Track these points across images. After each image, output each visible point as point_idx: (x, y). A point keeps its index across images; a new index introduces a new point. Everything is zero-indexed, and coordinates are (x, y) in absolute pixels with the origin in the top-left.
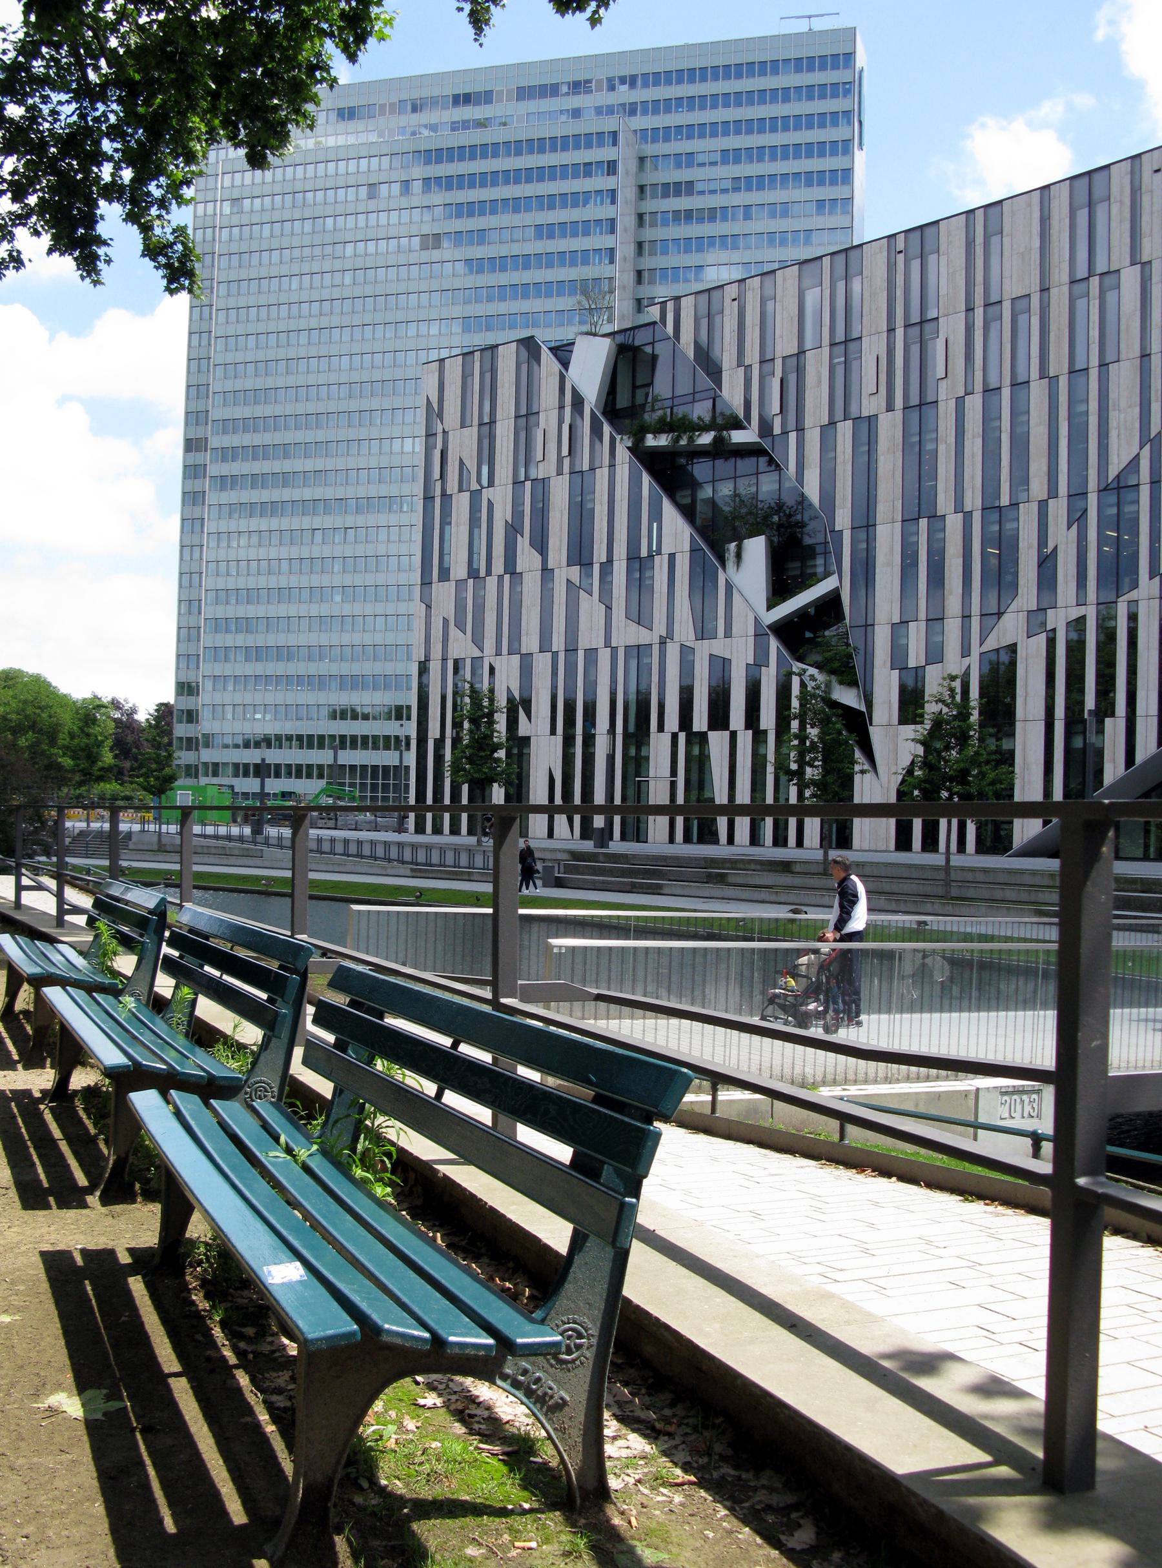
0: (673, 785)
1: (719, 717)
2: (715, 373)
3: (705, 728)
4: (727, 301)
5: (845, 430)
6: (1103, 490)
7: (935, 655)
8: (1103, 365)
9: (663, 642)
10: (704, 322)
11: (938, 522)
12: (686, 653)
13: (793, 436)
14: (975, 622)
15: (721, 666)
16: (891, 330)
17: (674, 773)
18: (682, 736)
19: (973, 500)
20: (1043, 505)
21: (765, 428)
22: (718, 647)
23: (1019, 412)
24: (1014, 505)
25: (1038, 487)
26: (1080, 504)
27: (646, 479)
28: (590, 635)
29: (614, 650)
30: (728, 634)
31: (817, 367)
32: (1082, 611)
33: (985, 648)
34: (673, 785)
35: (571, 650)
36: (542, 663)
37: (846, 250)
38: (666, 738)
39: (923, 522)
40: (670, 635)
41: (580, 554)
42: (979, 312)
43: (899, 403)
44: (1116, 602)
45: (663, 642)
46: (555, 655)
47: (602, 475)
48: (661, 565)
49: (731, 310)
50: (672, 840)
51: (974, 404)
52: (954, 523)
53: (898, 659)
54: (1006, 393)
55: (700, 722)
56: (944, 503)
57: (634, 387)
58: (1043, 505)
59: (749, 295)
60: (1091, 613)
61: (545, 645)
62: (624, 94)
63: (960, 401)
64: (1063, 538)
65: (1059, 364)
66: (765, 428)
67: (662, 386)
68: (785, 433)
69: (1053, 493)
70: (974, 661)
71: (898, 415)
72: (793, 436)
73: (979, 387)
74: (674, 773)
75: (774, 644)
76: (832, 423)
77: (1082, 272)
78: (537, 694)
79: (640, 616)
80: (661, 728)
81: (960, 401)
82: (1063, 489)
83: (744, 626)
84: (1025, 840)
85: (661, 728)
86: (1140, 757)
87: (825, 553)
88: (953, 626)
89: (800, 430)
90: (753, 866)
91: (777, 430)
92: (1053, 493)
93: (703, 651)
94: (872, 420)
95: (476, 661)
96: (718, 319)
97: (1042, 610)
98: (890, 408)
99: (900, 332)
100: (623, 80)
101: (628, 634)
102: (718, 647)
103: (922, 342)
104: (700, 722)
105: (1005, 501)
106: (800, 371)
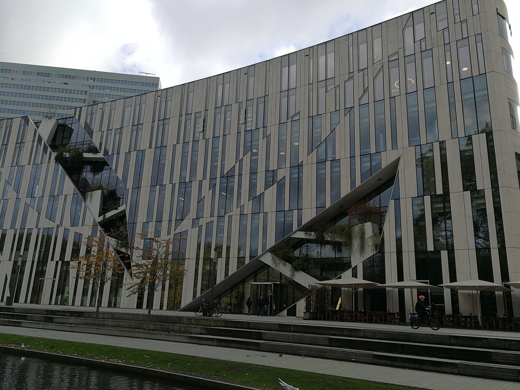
0: (54, 281)
2: (91, 133)
3: (69, 260)
4: (98, 109)
5: (134, 154)
6: (222, 177)
7: (158, 233)
8: (224, 135)
9: (58, 227)
10: (89, 116)
11: (162, 186)
12: (66, 230)
13: (115, 156)
14: (173, 222)
15: (78, 236)
16: (153, 121)
17: (55, 277)
18: (60, 263)
19: (176, 180)
20: (201, 182)
21: (106, 153)
22: (78, 229)
23: (194, 151)
24: (191, 182)
25: (199, 175)
26: (214, 182)
27: (61, 168)
28: (31, 224)
29: (39, 229)
30: (83, 225)
31: (127, 132)
32: (212, 219)
33: (176, 232)
34: (54, 281)
35: (22, 229)
37: (141, 95)
38: (54, 263)
39: (158, 187)
40: (61, 224)
41: (31, 195)
42: (184, 117)
43: (153, 146)
44: (224, 216)
45: (58, 227)
46: (16, 230)
47: (45, 166)
48: (62, 198)
49: (99, 112)
50: (26, 302)
51: (179, 147)
52: (169, 188)
53: (144, 236)
54: (191, 144)
55: (68, 257)
56: (166, 180)
57: (63, 138)
58: (201, 182)
59: (106, 108)
60: (215, 219)
62: (91, 82)
63: (175, 146)
64: (206, 192)
65: (209, 134)
66: (106, 153)
67: (73, 139)
68: (113, 154)
69: (204, 177)
70: (172, 236)
71: (153, 149)
72: (115, 156)
73: (181, 141)
74: (55, 277)
75: (99, 228)
76: (130, 152)
77: (219, 105)
78: (6, 245)
79: (51, 217)
81: (175, 146)
82: (208, 177)
83: (89, 222)
84: (186, 305)
86: (230, 274)
87: (123, 198)
88: (165, 224)
89: (118, 154)
90: (67, 314)
91: (110, 154)
93: (73, 230)
94: (143, 151)
96: (94, 115)
97: (198, 218)
98: (150, 147)
99: (156, 122)
100: (91, 79)
101: (45, 223)
102: (78, 229)
103: (164, 125)
104: (68, 257)
105: (187, 180)
106: (121, 134)
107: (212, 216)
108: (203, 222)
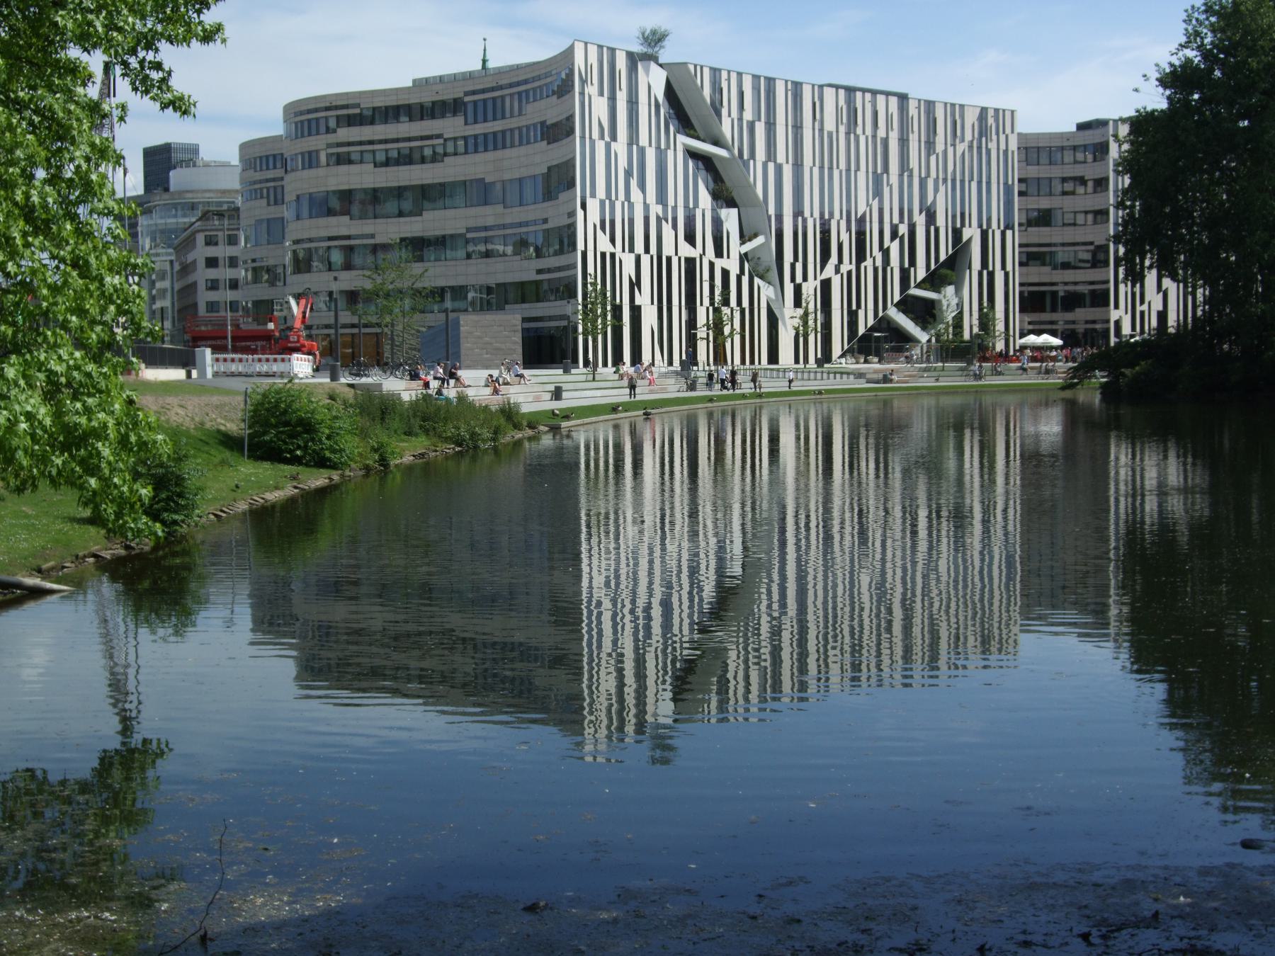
1: (726, 302)
9: (701, 256)
12: (712, 265)
15: (725, 273)
18: (711, 308)
19: (817, 214)
28: (668, 250)
29: (680, 259)
36: (645, 260)
53: (793, 279)
56: (807, 213)
60: (853, 267)
61: (647, 250)
64: (845, 237)
69: (841, 218)
70: (818, 283)
80: (701, 304)
85: (701, 304)
92: (841, 218)
95: (613, 256)
101: (686, 250)
107: (851, 263)
108: (845, 268)
